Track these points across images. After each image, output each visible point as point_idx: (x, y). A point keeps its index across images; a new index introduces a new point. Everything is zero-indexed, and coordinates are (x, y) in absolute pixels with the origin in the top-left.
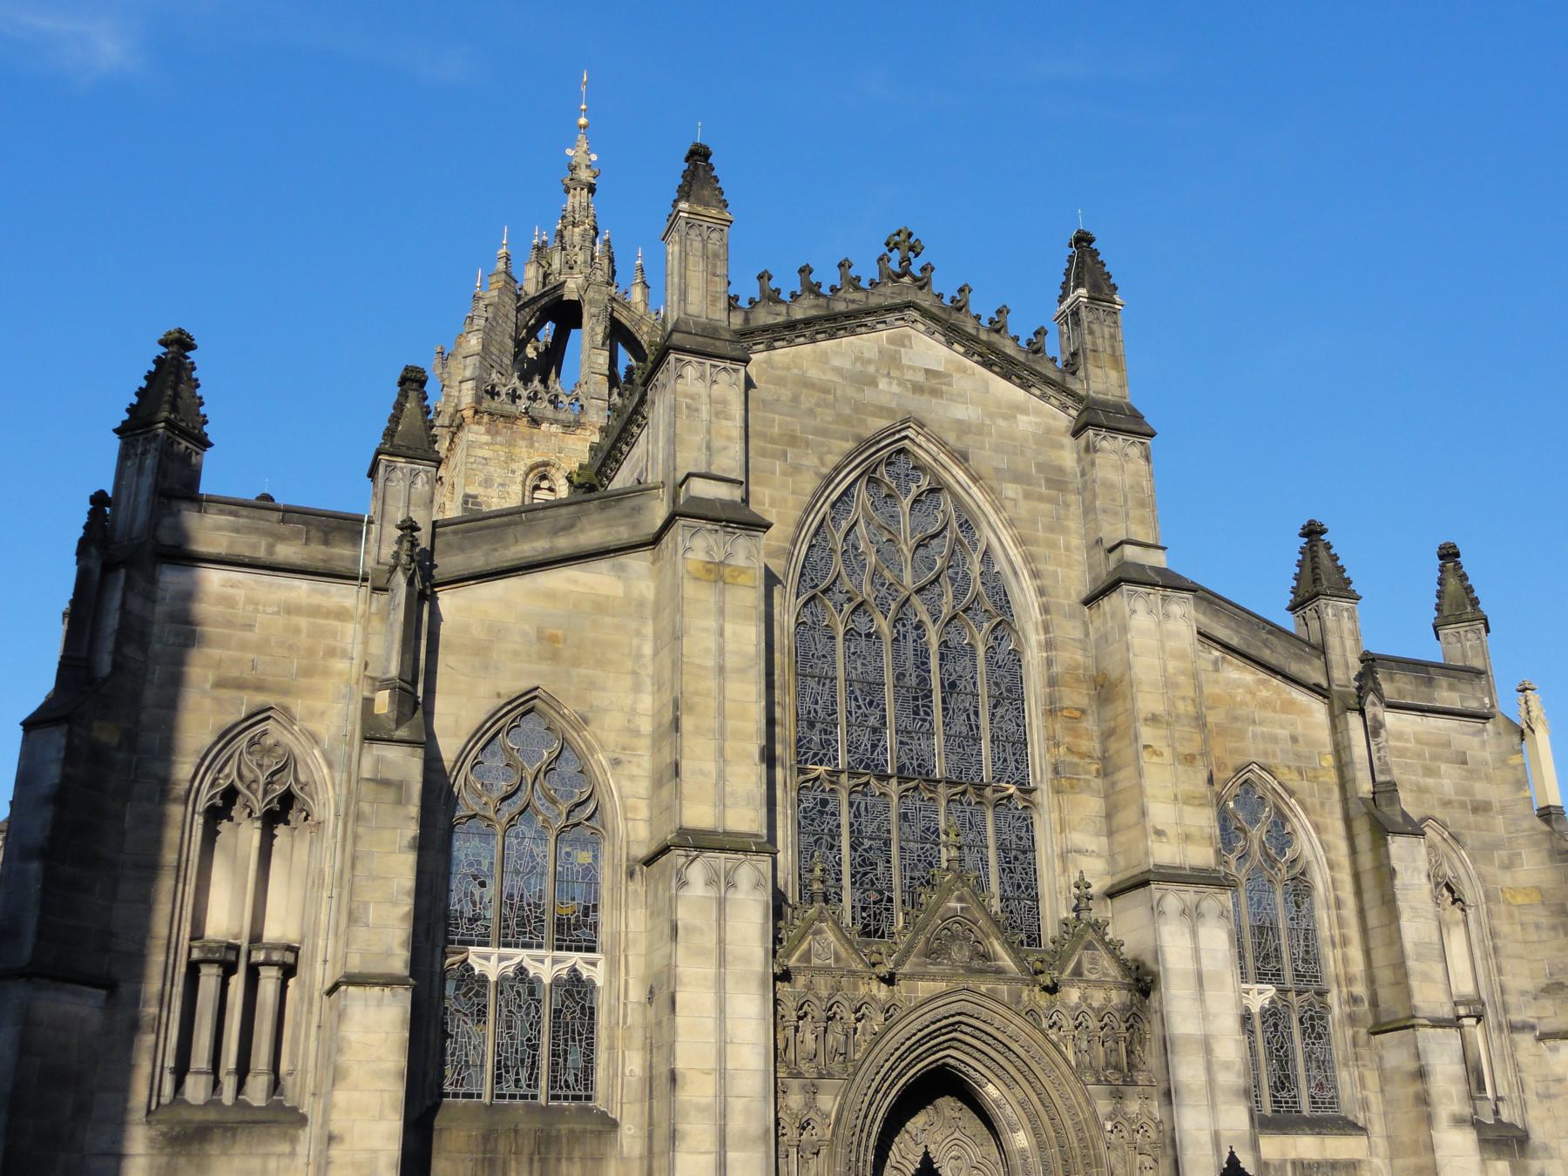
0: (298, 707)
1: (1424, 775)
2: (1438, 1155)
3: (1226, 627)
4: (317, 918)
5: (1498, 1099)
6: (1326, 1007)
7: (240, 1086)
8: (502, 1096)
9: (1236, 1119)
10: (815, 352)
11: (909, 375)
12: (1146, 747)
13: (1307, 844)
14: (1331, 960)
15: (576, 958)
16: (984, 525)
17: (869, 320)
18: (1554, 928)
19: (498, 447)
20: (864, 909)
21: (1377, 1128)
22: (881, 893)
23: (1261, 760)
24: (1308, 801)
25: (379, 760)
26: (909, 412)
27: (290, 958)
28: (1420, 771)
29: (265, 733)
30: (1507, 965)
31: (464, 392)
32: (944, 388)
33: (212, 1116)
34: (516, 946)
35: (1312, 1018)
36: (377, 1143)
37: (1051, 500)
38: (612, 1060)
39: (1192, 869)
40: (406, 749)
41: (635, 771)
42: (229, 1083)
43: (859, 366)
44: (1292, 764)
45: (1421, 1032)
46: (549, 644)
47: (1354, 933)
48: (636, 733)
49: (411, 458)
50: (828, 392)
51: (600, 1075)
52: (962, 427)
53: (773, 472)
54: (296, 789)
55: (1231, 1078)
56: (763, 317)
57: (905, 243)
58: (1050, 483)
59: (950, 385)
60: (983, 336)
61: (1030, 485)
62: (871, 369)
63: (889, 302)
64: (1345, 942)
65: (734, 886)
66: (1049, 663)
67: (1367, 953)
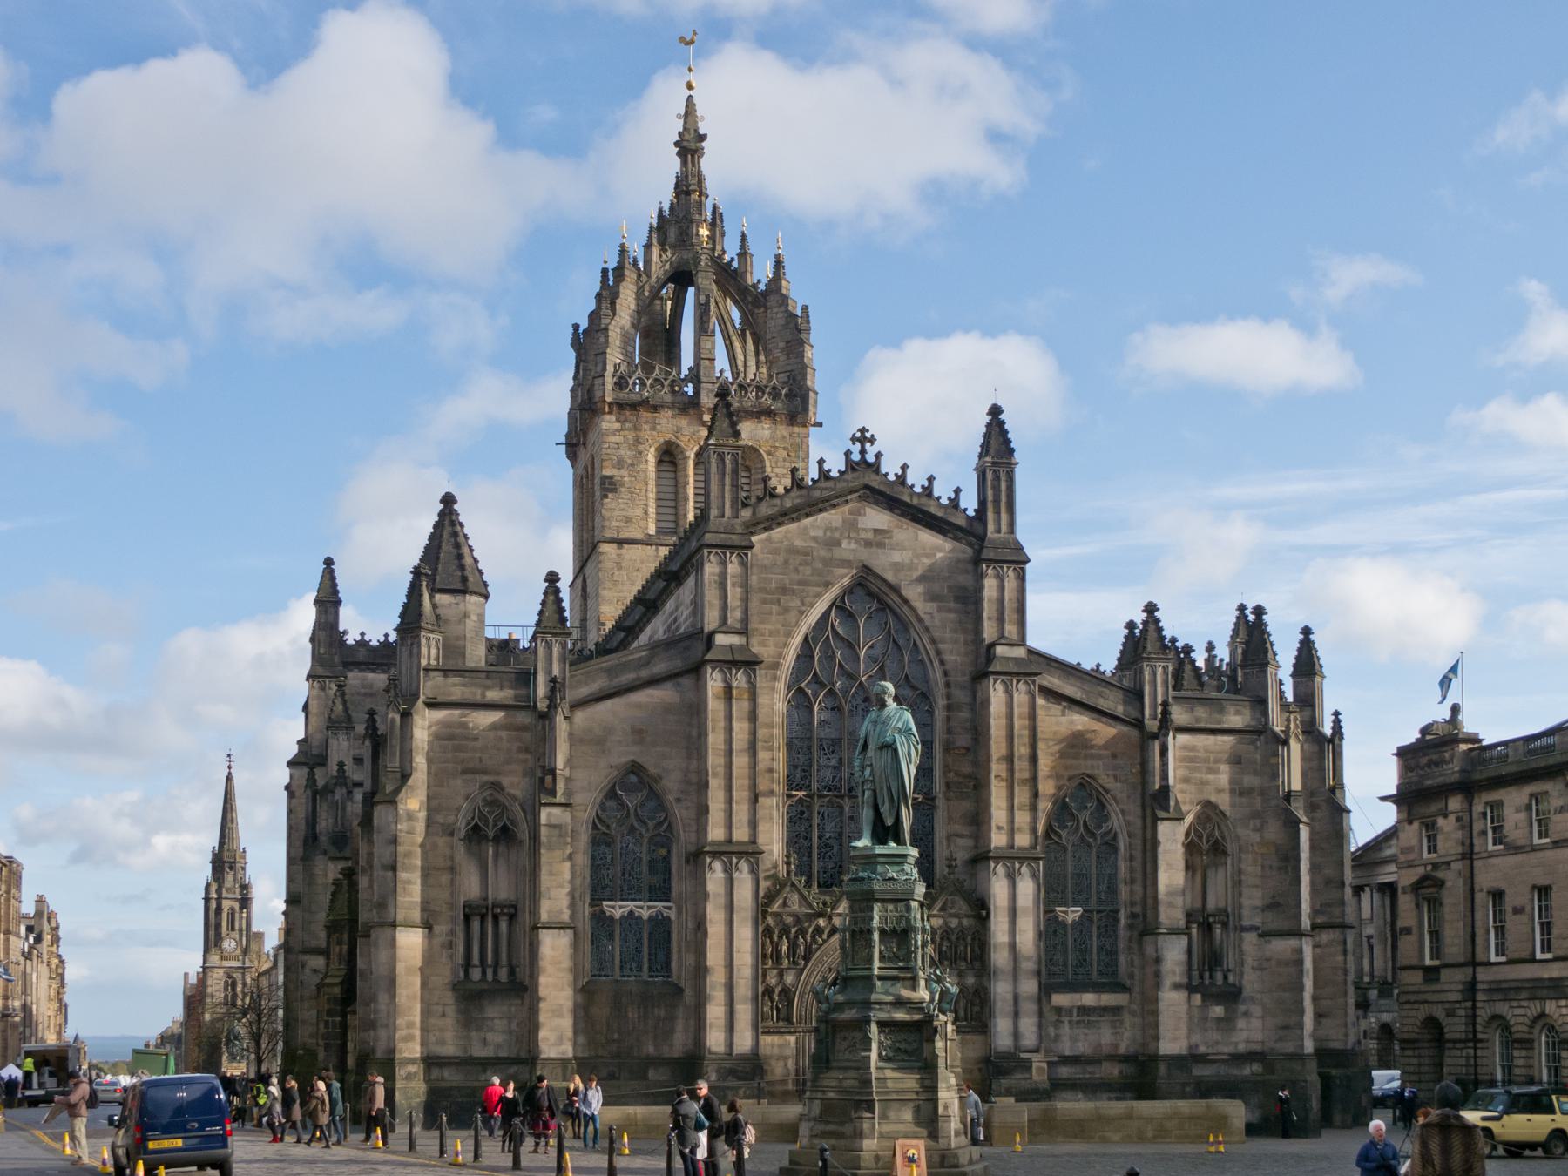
0: (505, 781)
1: (1207, 773)
2: (1162, 1006)
3: (1072, 685)
4: (524, 893)
5: (1229, 970)
6: (1117, 920)
7: (495, 973)
8: (624, 976)
9: (1029, 987)
10: (798, 527)
11: (863, 535)
12: (996, 777)
13: (1116, 821)
14: (1123, 890)
15: (660, 905)
16: (912, 630)
17: (835, 502)
18: (1280, 868)
19: (626, 433)
20: (825, 873)
21: (1137, 989)
22: (835, 863)
23: (1088, 772)
24: (1119, 796)
25: (549, 815)
26: (862, 561)
27: (512, 910)
28: (1204, 770)
29: (491, 795)
30: (1245, 891)
31: (596, 387)
32: (887, 541)
33: (485, 986)
34: (627, 900)
35: (1106, 926)
36: (562, 1002)
37: (955, 611)
38: (680, 958)
39: (1020, 848)
40: (564, 808)
41: (689, 804)
42: (490, 972)
43: (828, 534)
44: (1110, 772)
45: (1161, 938)
46: (638, 734)
47: (1138, 876)
48: (688, 782)
49: (555, 634)
50: (807, 554)
51: (674, 965)
52: (898, 567)
53: (771, 613)
54: (508, 824)
55: (1028, 965)
56: (766, 509)
57: (863, 438)
58: (957, 599)
59: (891, 538)
60: (915, 501)
61: (941, 602)
62: (837, 535)
63: (851, 485)
64: (1132, 881)
65: (741, 872)
66: (948, 719)
67: (1145, 887)
